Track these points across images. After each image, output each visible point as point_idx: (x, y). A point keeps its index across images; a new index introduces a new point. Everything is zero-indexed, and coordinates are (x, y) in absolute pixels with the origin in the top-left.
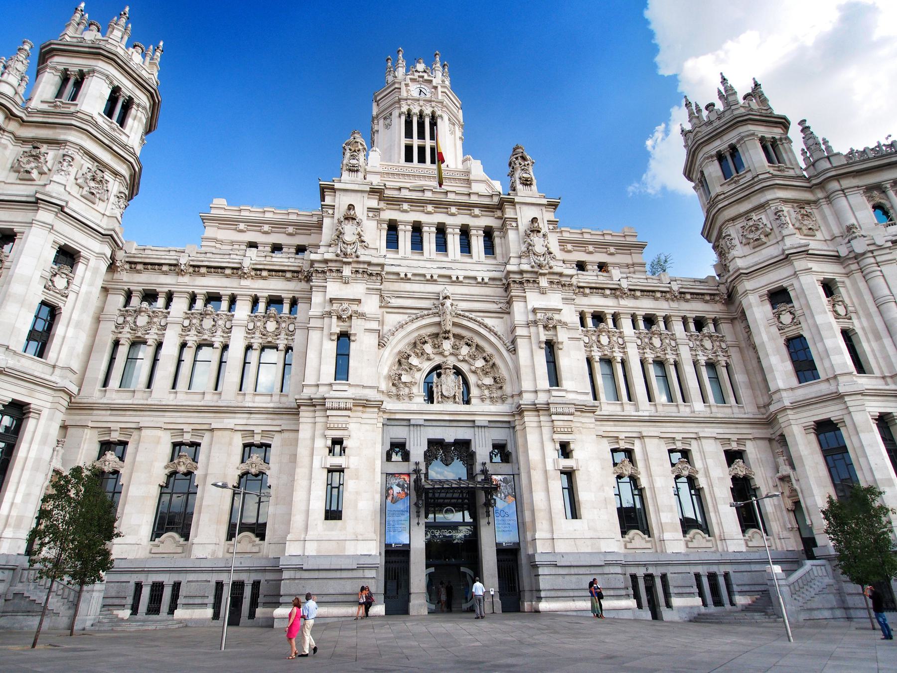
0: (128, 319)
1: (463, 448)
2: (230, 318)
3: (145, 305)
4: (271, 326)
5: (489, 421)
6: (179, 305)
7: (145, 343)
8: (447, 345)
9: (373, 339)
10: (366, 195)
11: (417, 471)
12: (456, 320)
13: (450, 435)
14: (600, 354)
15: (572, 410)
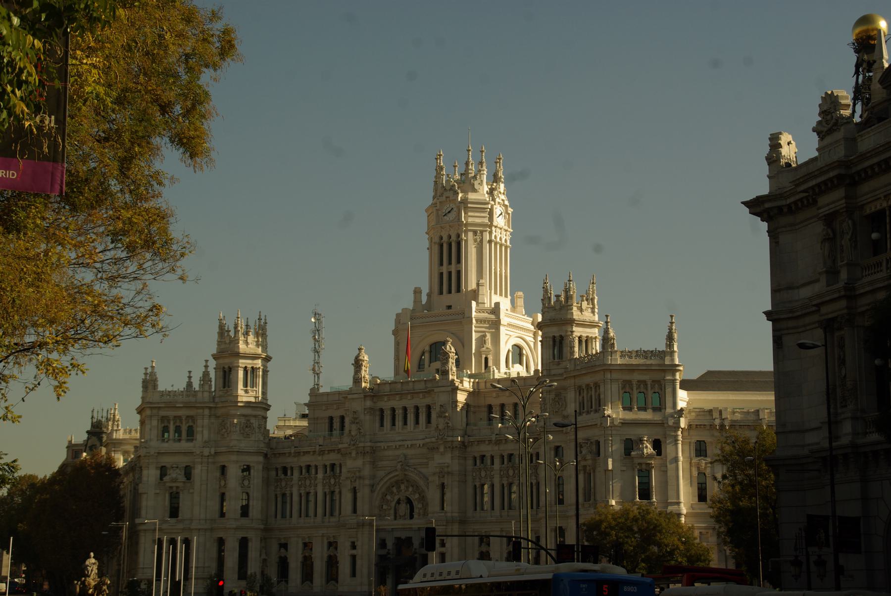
0: (279, 483)
1: (409, 540)
2: (316, 478)
3: (283, 476)
4: (332, 481)
5: (419, 528)
6: (296, 474)
7: (286, 494)
8: (403, 487)
9: (367, 491)
10: (363, 400)
11: (388, 553)
12: (406, 473)
13: (403, 535)
14: (479, 483)
15: (445, 524)
